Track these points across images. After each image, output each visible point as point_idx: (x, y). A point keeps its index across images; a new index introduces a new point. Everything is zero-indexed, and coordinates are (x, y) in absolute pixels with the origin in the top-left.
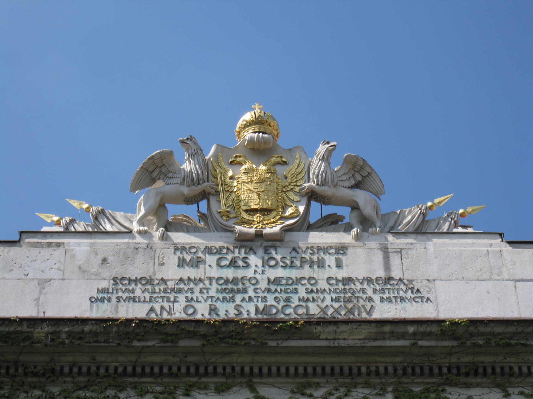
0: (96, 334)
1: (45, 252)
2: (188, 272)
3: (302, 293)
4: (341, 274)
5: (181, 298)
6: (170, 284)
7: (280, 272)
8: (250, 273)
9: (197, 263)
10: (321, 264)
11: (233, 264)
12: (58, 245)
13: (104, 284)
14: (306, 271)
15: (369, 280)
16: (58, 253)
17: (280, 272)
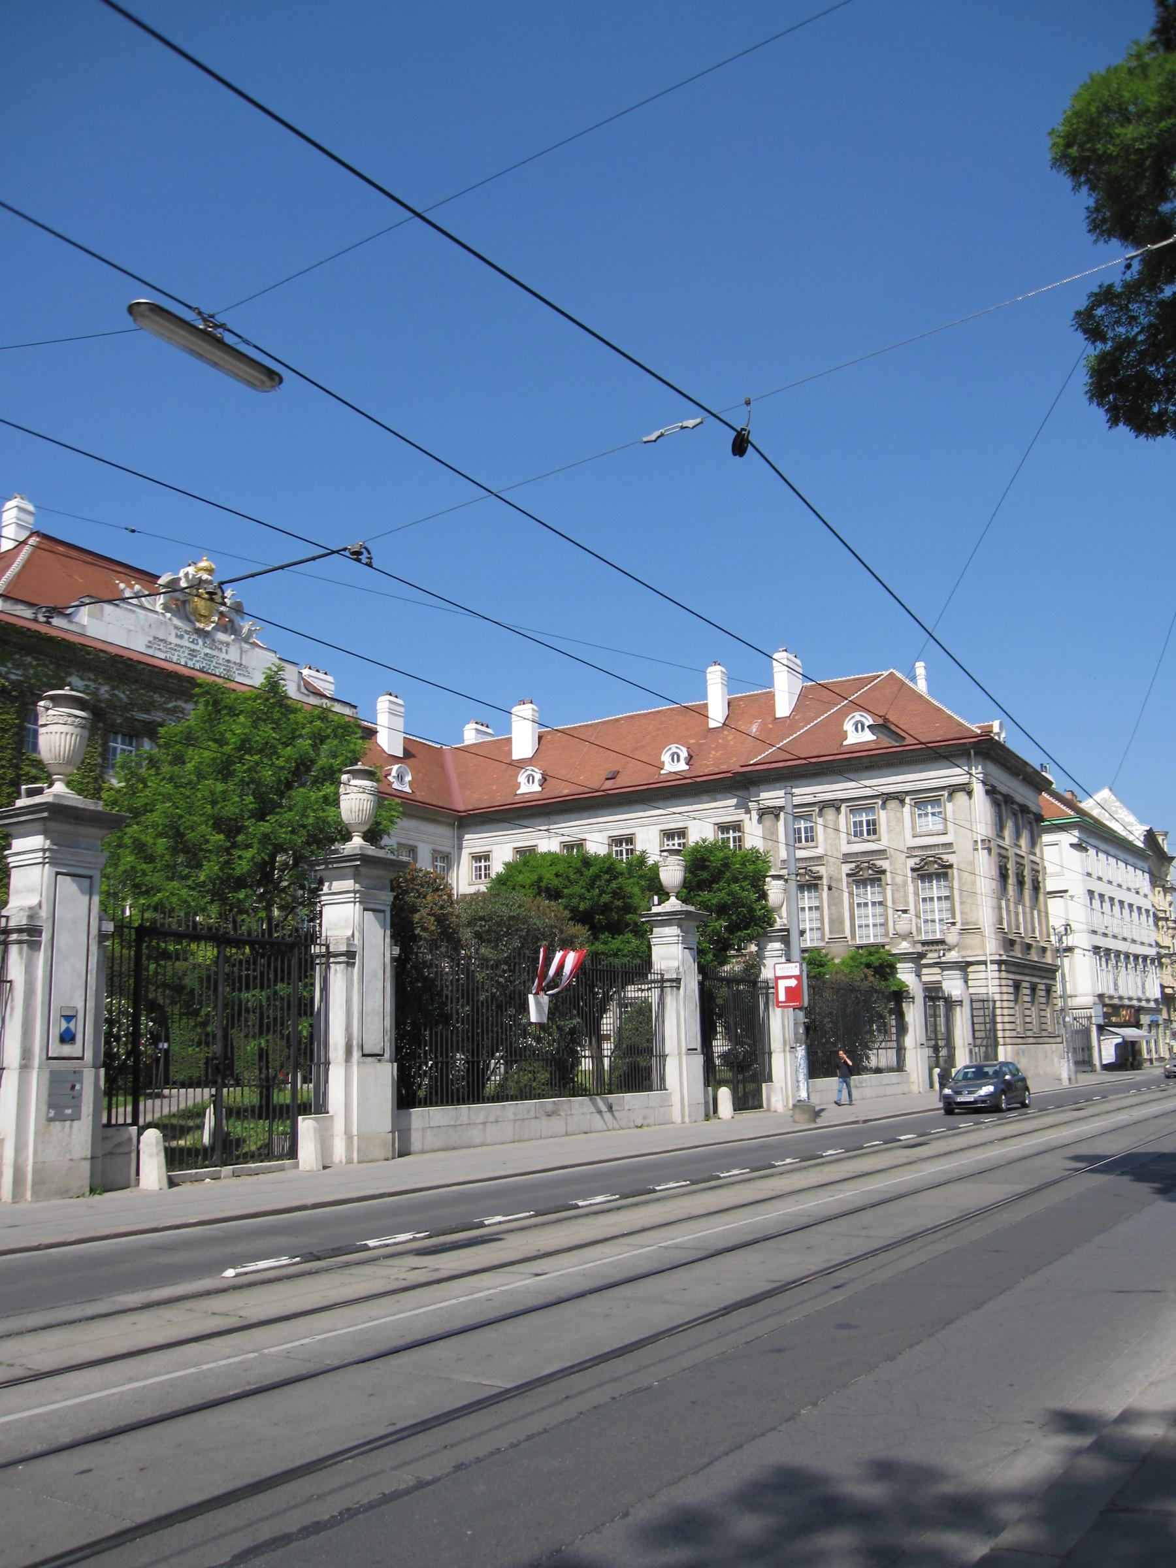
0: (158, 673)
1: (130, 615)
2: (178, 641)
3: (214, 664)
4: (227, 657)
5: (177, 653)
6: (172, 646)
7: (207, 651)
8: (197, 648)
9: (181, 637)
10: (220, 650)
11: (193, 642)
12: (134, 612)
13: (151, 639)
14: (215, 653)
15: (235, 663)
16: (133, 616)
17: (207, 651)
